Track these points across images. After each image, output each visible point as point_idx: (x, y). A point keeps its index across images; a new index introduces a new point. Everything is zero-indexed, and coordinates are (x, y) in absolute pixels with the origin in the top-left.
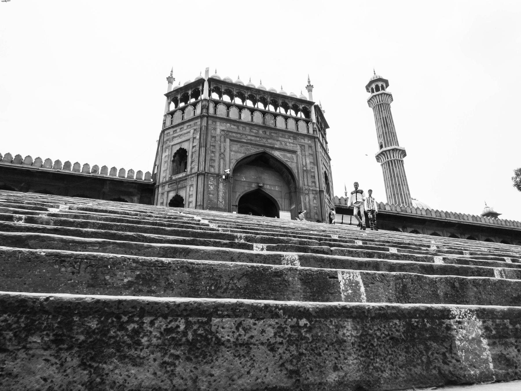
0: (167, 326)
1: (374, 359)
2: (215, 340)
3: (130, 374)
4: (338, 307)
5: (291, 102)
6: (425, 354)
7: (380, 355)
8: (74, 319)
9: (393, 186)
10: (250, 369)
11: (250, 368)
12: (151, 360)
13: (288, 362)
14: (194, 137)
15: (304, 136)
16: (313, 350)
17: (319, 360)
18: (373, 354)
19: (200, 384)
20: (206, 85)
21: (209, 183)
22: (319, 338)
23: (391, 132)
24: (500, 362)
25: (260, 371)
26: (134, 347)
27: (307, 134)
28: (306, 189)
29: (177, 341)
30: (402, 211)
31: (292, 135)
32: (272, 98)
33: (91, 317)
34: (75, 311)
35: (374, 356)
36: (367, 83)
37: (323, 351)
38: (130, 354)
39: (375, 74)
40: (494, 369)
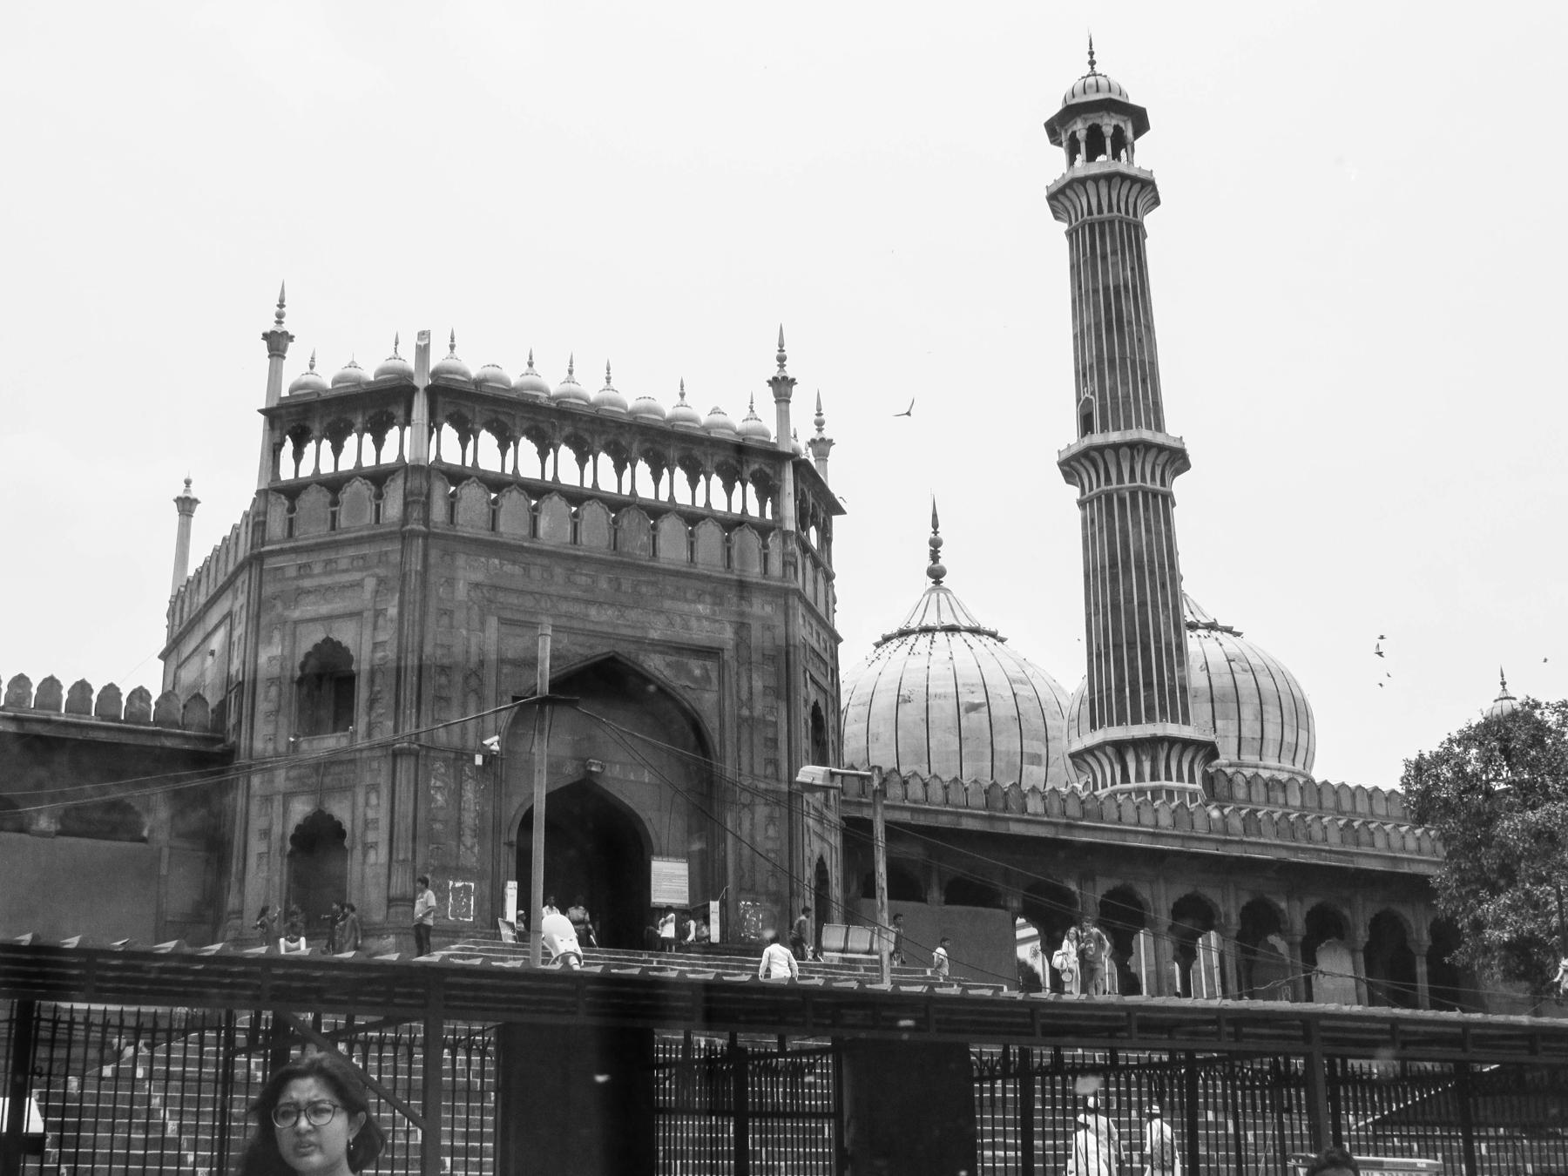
5: (712, 455)
9: (1115, 607)
23: (1133, 362)
31: (709, 587)
32: (648, 445)
36: (1057, 107)
39: (1092, 63)
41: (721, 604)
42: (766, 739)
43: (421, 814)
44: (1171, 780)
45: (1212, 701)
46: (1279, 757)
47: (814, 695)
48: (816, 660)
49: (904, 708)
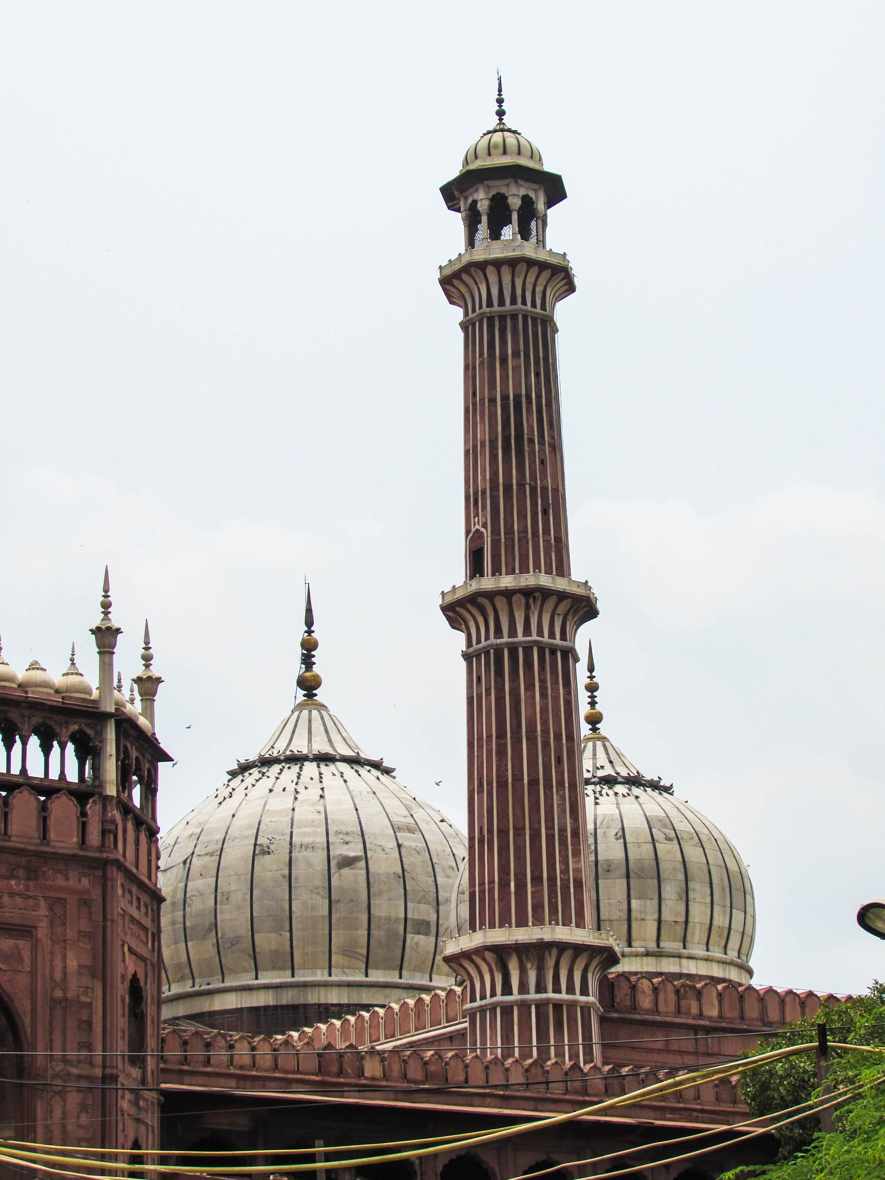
5: (29, 717)
9: (502, 784)
15: (68, 860)
23: (533, 489)
28: (56, 1076)
31: (23, 861)
36: (454, 171)
39: (501, 113)
42: (81, 1022)
44: (560, 992)
45: (628, 877)
46: (707, 944)
47: (131, 966)
48: (135, 928)
49: (261, 861)
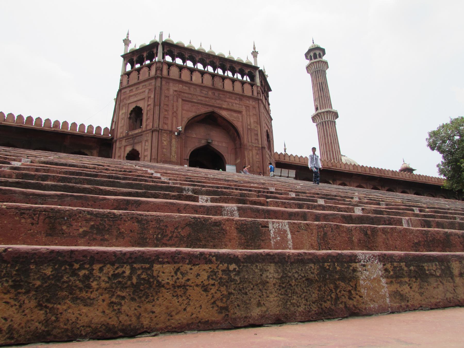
0: (114, 271)
1: (291, 297)
2: (156, 283)
3: (81, 313)
4: (263, 254)
5: (238, 66)
6: (334, 291)
7: (297, 293)
8: (30, 267)
9: (326, 144)
10: (186, 307)
11: (186, 305)
12: (100, 302)
13: (218, 300)
14: (149, 96)
16: (240, 290)
17: (245, 298)
18: (291, 293)
19: (142, 319)
20: (160, 48)
21: (163, 139)
22: (246, 280)
23: (326, 96)
24: (395, 297)
25: (195, 308)
26: (85, 290)
27: (251, 96)
28: (250, 146)
29: (123, 285)
30: (333, 166)
31: (238, 97)
32: (221, 63)
33: (46, 265)
34: (32, 259)
35: (291, 294)
36: (306, 51)
37: (249, 291)
38: (81, 296)
39: (313, 43)
40: (390, 303)
41: (242, 101)
42: (255, 134)
43: (159, 147)
